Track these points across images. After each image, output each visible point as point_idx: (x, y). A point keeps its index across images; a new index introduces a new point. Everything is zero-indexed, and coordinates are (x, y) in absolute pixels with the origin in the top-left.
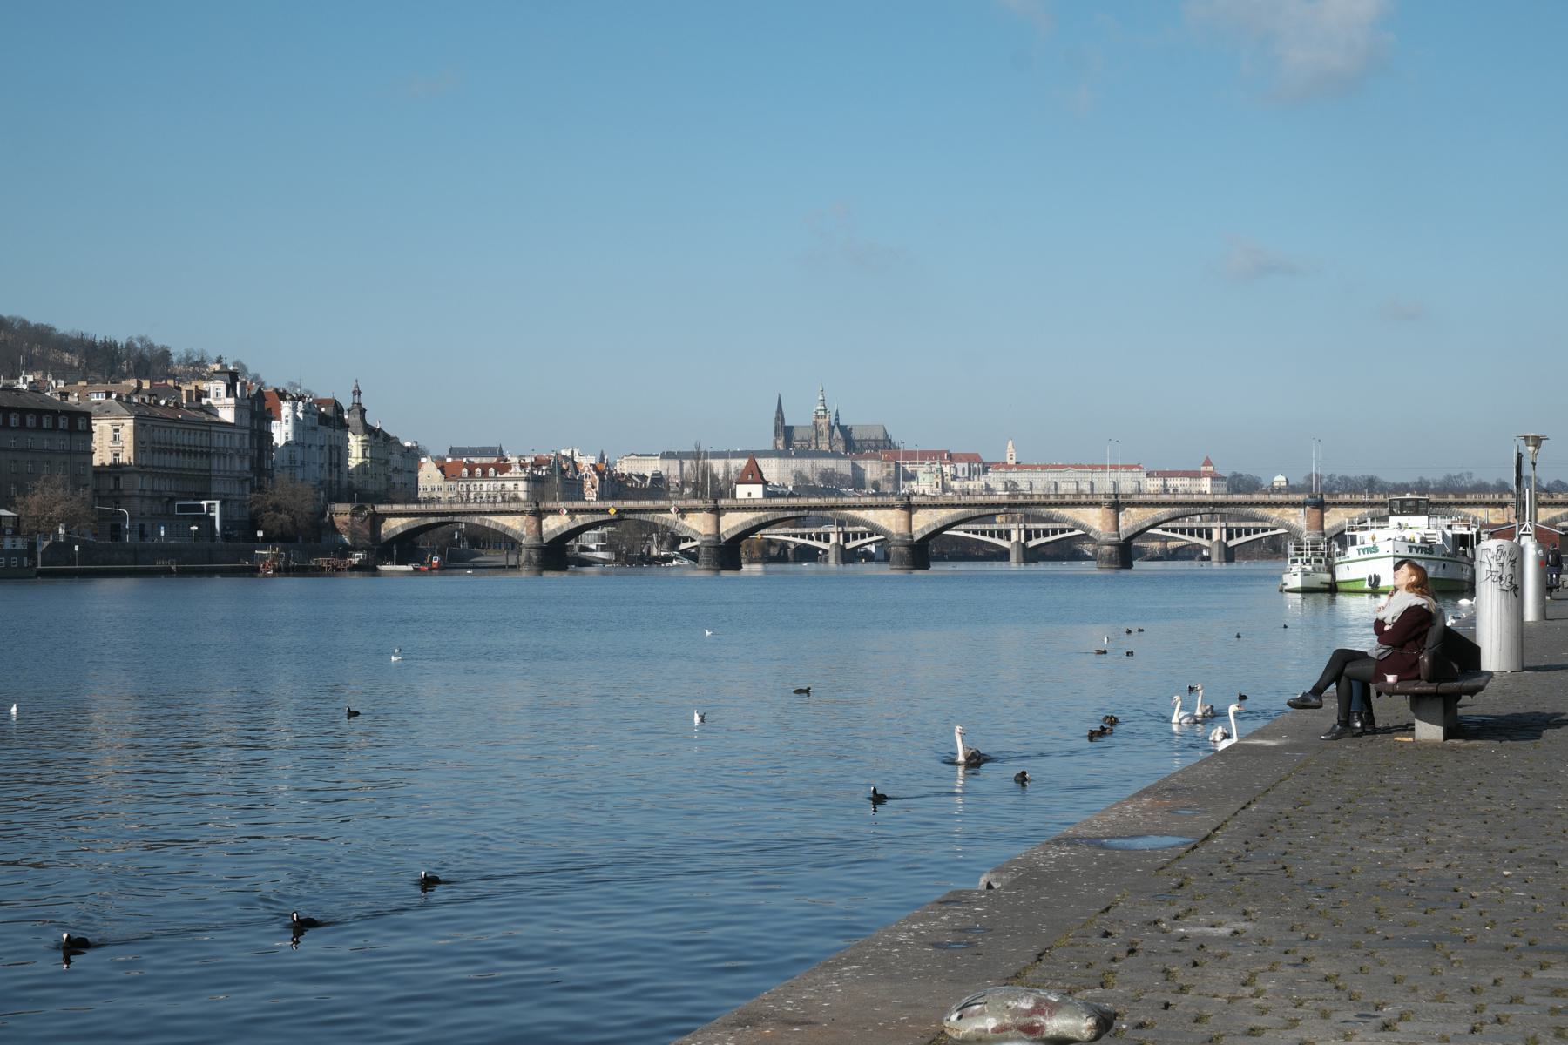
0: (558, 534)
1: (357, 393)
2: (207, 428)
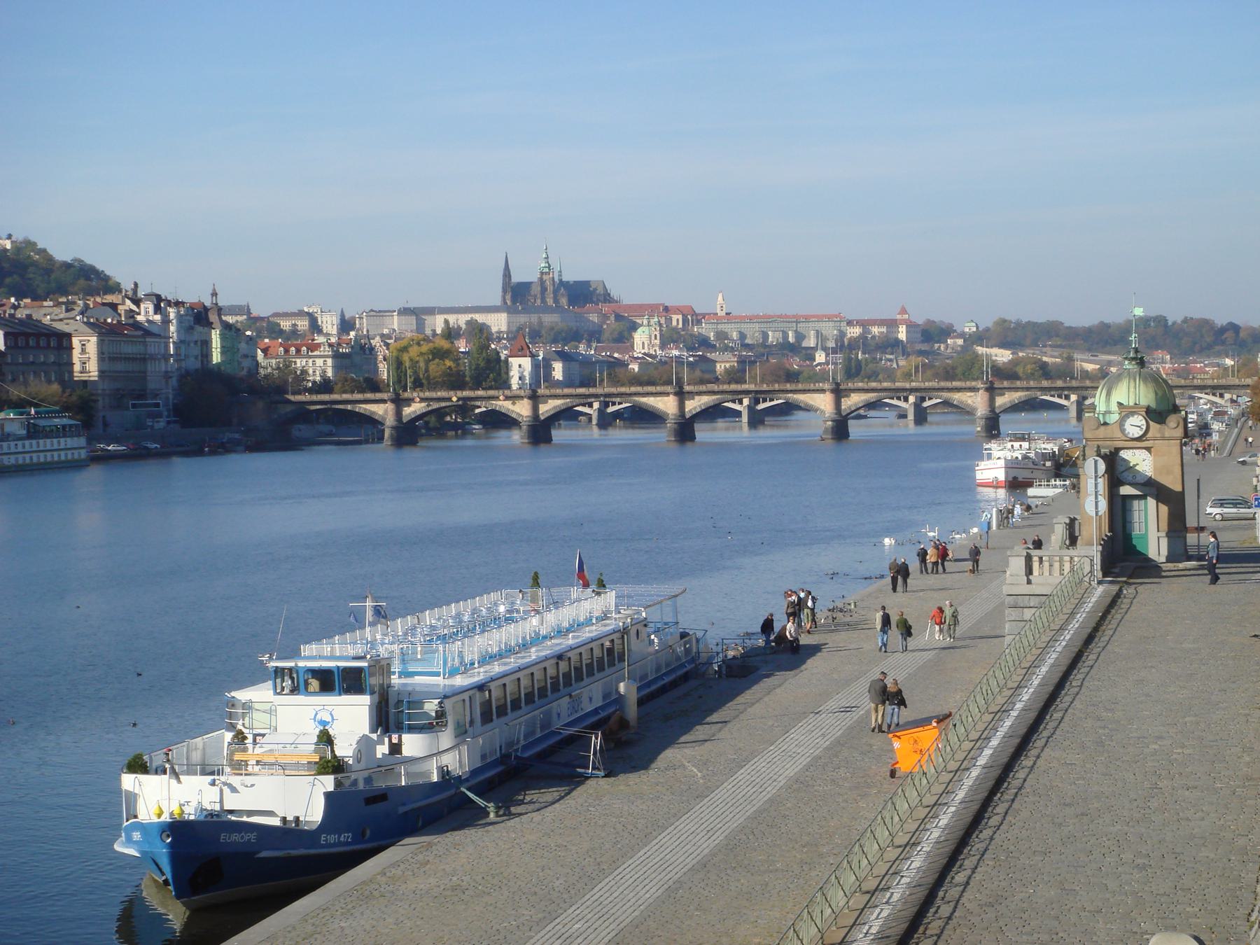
0: (413, 417)
1: (214, 294)
2: (143, 340)
